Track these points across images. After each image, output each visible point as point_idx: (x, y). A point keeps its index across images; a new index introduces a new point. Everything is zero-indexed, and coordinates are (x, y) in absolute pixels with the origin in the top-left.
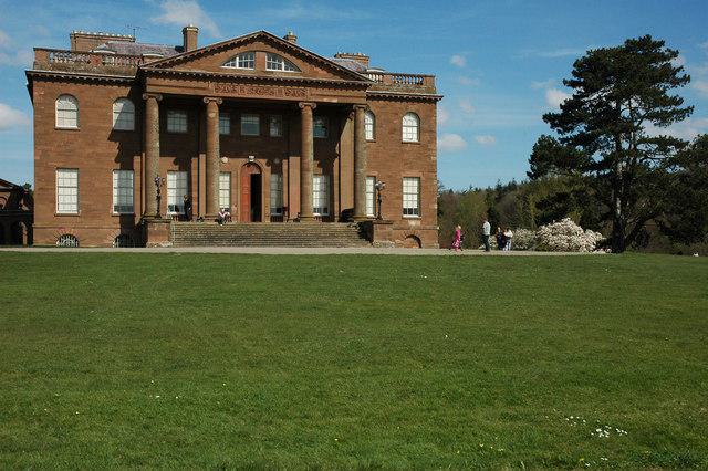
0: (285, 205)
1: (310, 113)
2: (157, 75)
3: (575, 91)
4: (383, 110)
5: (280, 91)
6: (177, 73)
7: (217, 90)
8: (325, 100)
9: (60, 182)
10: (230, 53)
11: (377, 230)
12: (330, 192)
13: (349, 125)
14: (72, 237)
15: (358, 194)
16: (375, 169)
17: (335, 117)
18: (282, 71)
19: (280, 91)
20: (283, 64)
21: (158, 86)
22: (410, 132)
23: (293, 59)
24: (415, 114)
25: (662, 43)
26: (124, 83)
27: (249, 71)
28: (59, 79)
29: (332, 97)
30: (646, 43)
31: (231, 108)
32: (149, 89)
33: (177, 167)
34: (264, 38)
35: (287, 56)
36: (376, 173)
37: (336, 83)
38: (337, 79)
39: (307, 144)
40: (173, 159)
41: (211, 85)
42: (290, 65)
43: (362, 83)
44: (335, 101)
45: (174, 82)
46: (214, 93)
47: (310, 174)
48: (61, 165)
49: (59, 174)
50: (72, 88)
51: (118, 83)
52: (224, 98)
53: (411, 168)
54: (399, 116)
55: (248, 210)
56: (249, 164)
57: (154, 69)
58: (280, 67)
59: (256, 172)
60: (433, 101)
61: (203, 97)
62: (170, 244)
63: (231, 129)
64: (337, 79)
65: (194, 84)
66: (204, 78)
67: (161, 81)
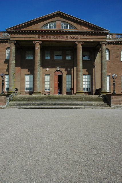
0: (73, 87)
1: (81, 46)
4: (112, 48)
5: (67, 37)
6: (22, 31)
8: (88, 40)
10: (45, 22)
11: (113, 99)
12: (92, 82)
13: (99, 55)
15: (103, 82)
16: (110, 72)
19: (67, 37)
20: (68, 26)
23: (73, 23)
29: (91, 39)
31: (46, 47)
33: (29, 73)
35: (70, 22)
36: (110, 74)
37: (92, 33)
39: (79, 60)
40: (28, 69)
41: (36, 36)
42: (72, 26)
43: (104, 32)
44: (92, 40)
45: (21, 36)
46: (38, 39)
47: (81, 74)
52: (42, 41)
56: (58, 71)
58: (67, 27)
59: (60, 74)
61: (33, 41)
62: (5, 106)
63: (51, 58)
65: (30, 36)
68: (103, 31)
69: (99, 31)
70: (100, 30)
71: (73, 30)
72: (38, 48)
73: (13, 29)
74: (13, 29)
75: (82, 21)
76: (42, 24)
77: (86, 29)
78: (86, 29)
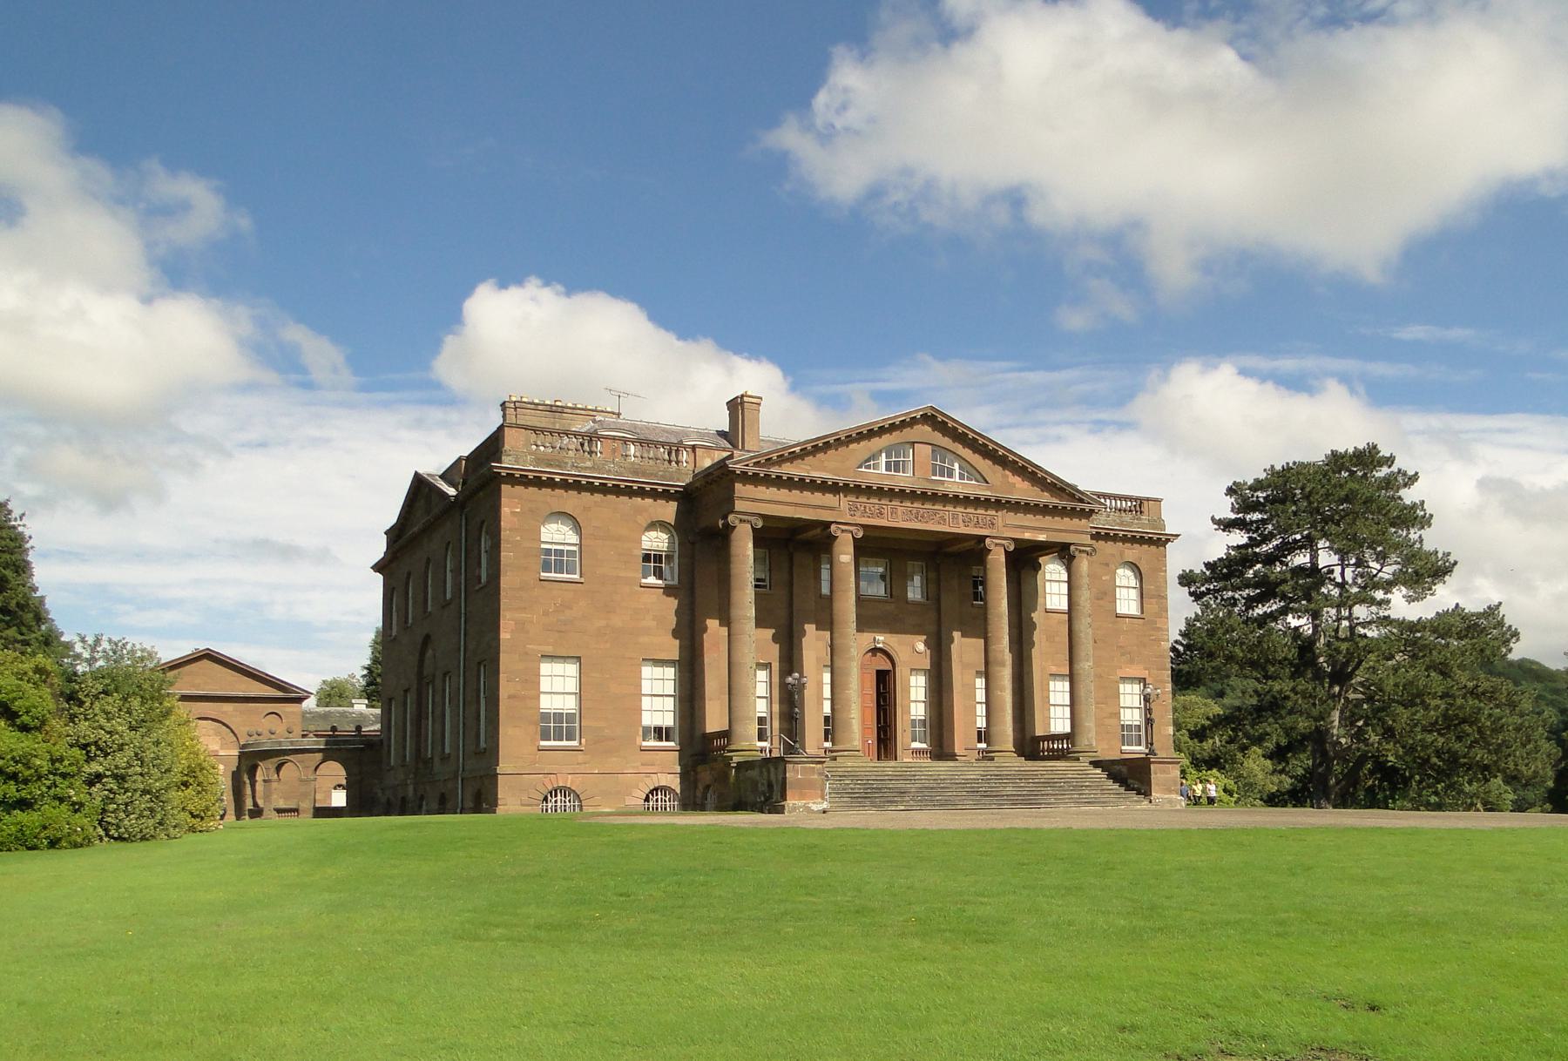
2: (755, 480)
3: (1239, 538)
5: (955, 517)
7: (853, 510)
8: (1027, 536)
9: (545, 685)
11: (1158, 775)
14: (565, 791)
17: (1024, 559)
18: (956, 483)
19: (955, 517)
20: (956, 466)
21: (754, 502)
22: (1127, 602)
23: (976, 459)
24: (1134, 567)
25: (1390, 461)
26: (666, 495)
27: (904, 480)
28: (551, 484)
29: (1037, 530)
30: (1367, 458)
32: (739, 506)
34: (932, 419)
35: (967, 453)
38: (1046, 498)
41: (844, 502)
42: (970, 470)
44: (1042, 537)
45: (782, 495)
48: (549, 650)
49: (546, 668)
50: (571, 501)
51: (654, 495)
53: (1131, 661)
54: (1109, 567)
55: (872, 740)
56: (875, 651)
57: (751, 470)
59: (888, 666)
60: (1160, 541)
62: (825, 805)
64: (1046, 498)
65: (818, 498)
66: (834, 488)
67: (763, 492)
68: (1081, 501)
69: (1069, 504)
70: (1072, 497)
71: (971, 488)
72: (845, 555)
73: (756, 464)
74: (756, 464)
75: (1011, 457)
76: (861, 449)
77: (1022, 490)
78: (1022, 490)
